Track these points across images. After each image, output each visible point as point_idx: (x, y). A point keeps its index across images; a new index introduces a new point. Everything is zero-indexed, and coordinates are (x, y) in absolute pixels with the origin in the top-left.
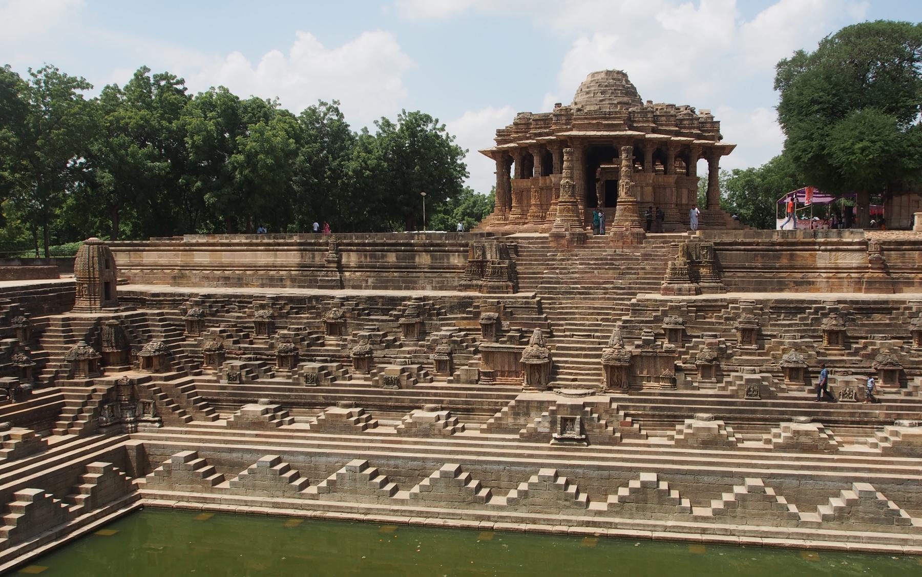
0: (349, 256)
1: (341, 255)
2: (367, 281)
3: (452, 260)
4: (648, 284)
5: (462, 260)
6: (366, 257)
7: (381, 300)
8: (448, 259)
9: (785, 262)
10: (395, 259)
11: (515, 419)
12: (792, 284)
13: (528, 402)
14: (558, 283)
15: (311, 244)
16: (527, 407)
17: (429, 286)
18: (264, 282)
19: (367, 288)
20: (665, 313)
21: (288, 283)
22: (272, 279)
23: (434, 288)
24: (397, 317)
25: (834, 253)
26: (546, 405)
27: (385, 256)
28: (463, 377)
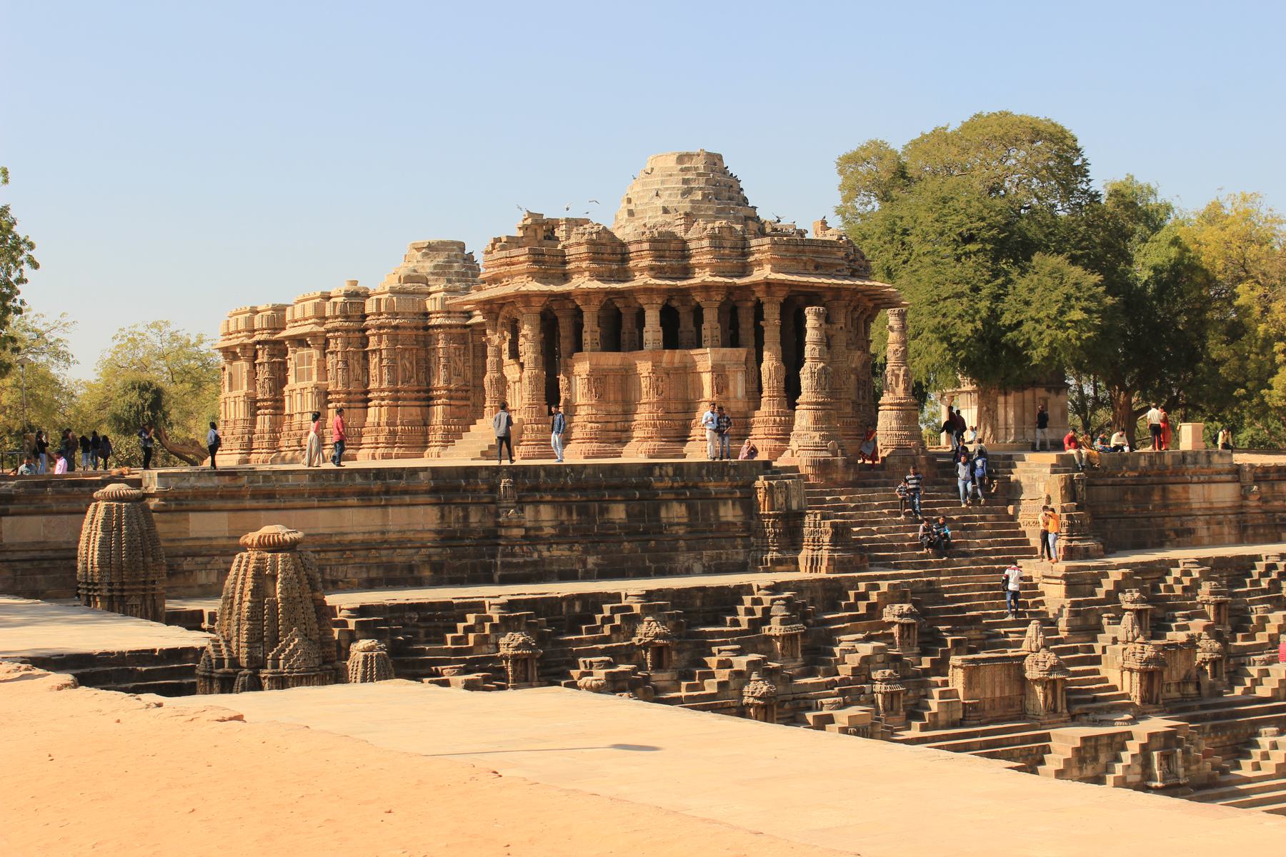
0: (537, 512)
1: (522, 510)
2: (585, 563)
3: (722, 512)
4: (1004, 543)
5: (739, 512)
6: (570, 513)
7: (701, 594)
8: (717, 511)
9: (1156, 498)
10: (623, 515)
11: (1081, 769)
12: (1172, 535)
13: (1097, 738)
14: (891, 548)
15: (457, 489)
16: (1096, 750)
17: (697, 567)
18: (373, 574)
19: (588, 576)
20: (1120, 587)
21: (427, 573)
22: (389, 567)
23: (708, 571)
24: (755, 625)
25: (1206, 486)
26: (1118, 739)
27: (607, 510)
28: (942, 717)
